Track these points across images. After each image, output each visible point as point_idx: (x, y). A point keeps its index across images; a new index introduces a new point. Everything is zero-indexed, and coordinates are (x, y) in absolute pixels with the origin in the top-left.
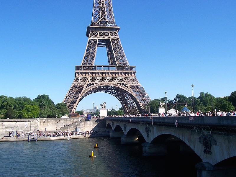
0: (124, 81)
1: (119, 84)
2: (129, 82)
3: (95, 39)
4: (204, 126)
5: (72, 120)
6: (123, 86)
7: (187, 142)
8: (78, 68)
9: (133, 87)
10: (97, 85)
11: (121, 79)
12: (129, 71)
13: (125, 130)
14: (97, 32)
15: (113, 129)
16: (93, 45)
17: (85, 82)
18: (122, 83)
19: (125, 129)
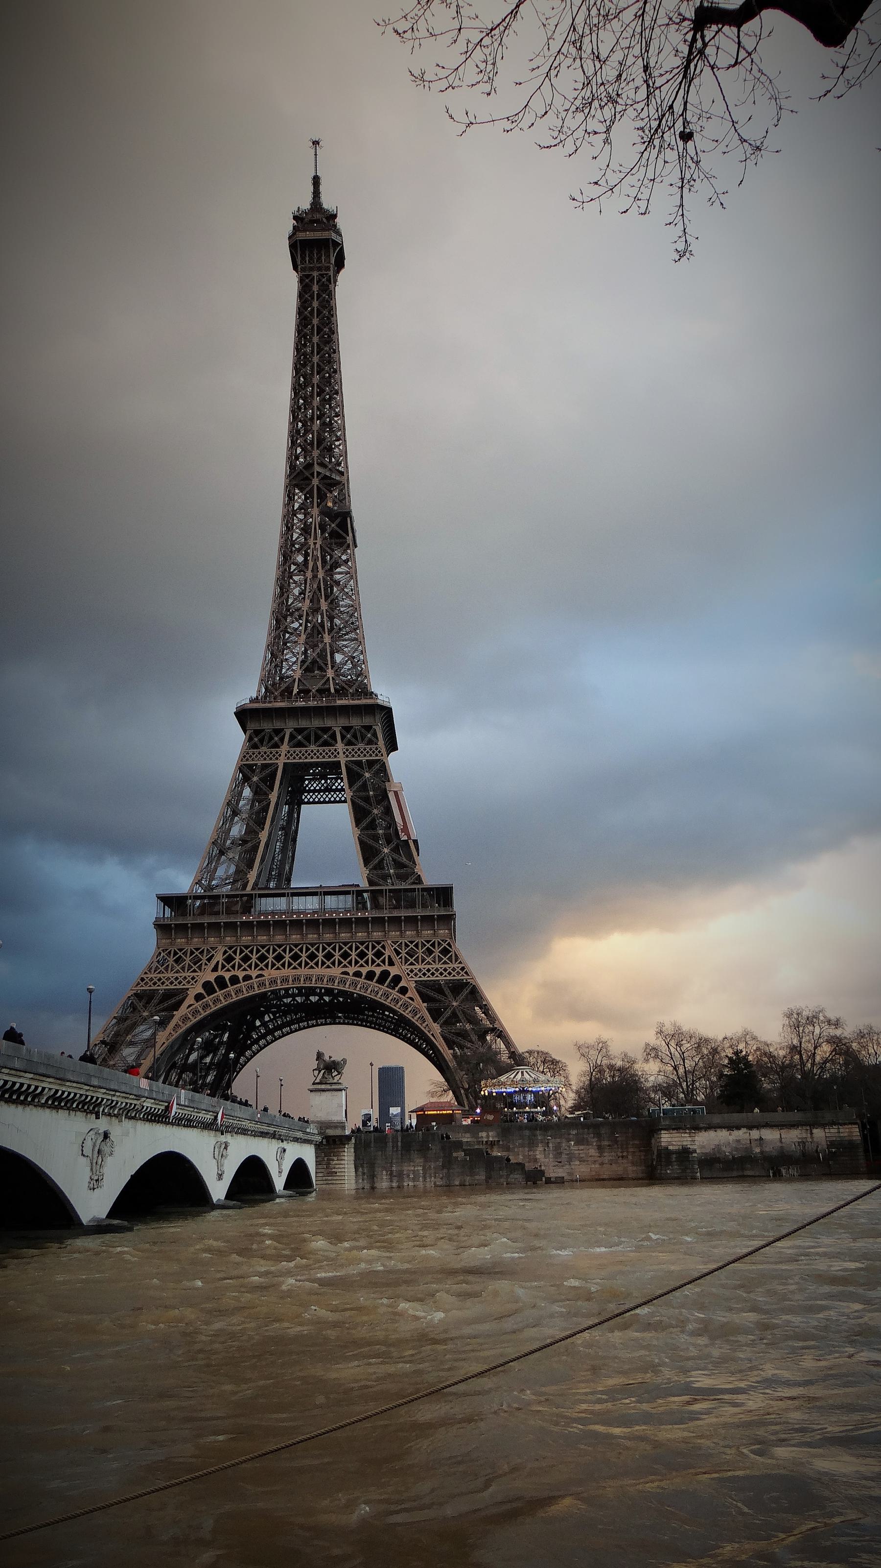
0: (391, 963)
1: (362, 980)
3: (271, 765)
6: (384, 988)
8: (172, 902)
11: (379, 954)
14: (278, 732)
17: (195, 974)
18: (378, 971)
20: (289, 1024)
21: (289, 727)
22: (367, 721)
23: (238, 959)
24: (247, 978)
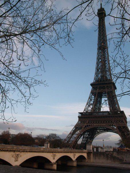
11: (111, 122)
20: (101, 132)
21: (98, 86)
24: (91, 125)
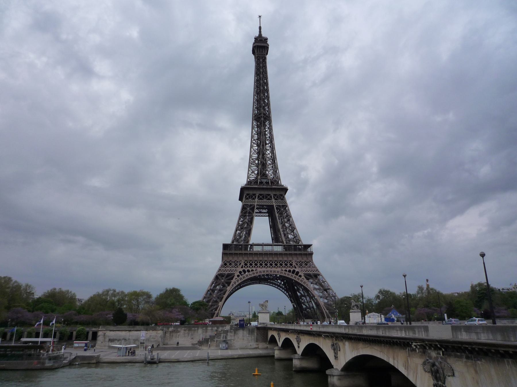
0: (295, 268)
2: (303, 269)
4: (430, 343)
5: (216, 328)
6: (294, 275)
7: (402, 369)
8: (226, 247)
9: (308, 277)
10: (254, 274)
11: (291, 265)
12: (303, 252)
13: (299, 347)
14: (254, 195)
15: (280, 344)
16: (249, 213)
18: (292, 270)
19: (299, 344)
21: (258, 193)
22: (282, 193)
23: (248, 265)
24: (252, 270)
